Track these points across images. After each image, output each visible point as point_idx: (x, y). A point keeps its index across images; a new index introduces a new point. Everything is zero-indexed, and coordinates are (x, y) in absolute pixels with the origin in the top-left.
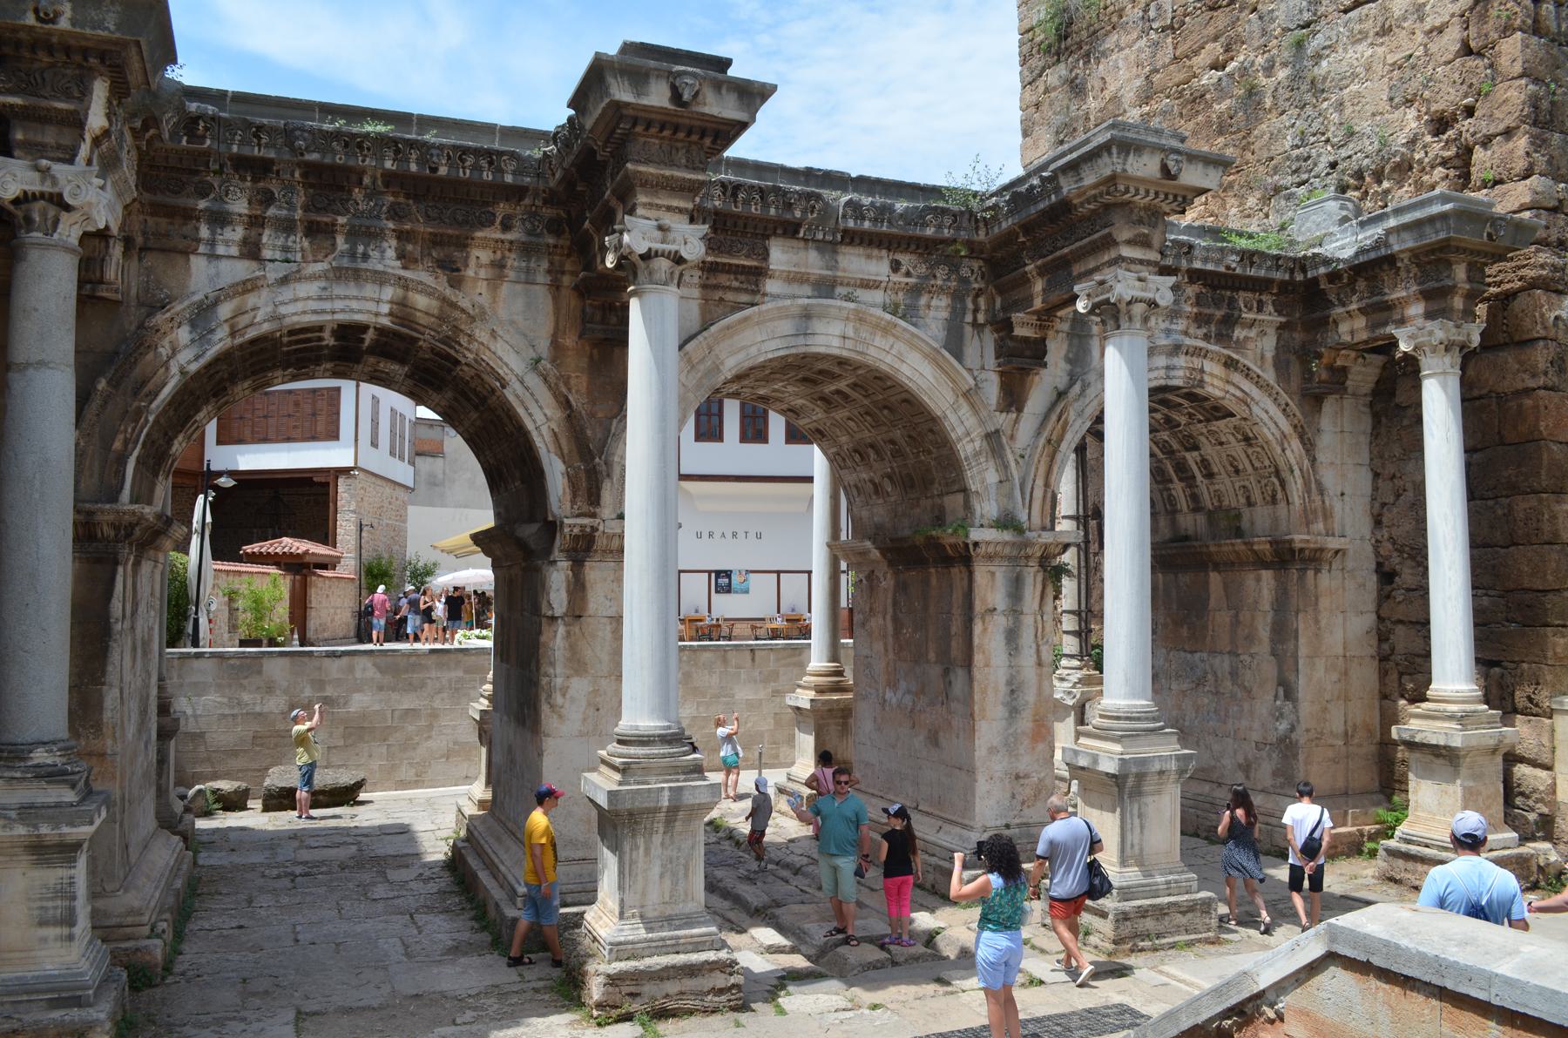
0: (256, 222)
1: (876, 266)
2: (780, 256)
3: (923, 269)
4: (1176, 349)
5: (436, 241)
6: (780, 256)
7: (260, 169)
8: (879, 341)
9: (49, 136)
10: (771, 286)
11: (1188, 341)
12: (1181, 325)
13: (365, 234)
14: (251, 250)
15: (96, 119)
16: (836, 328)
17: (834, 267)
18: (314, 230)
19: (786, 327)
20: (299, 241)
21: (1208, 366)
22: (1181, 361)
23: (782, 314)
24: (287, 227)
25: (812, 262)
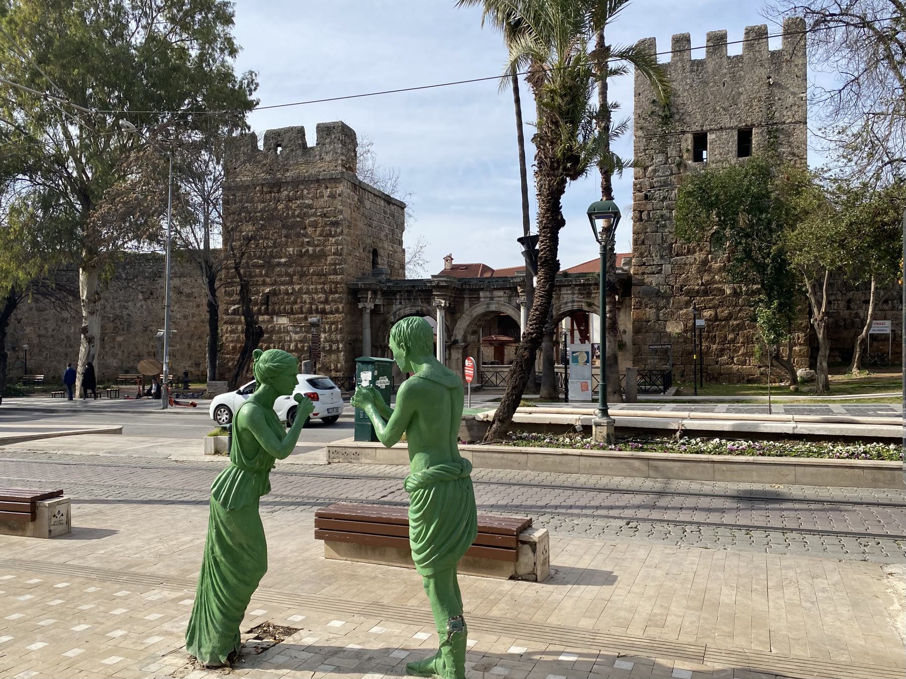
0: (401, 299)
1: (501, 293)
2: (482, 294)
3: (510, 293)
4: (573, 301)
5: (426, 299)
6: (482, 294)
7: (400, 291)
8: (503, 307)
9: (364, 300)
10: (481, 300)
11: (576, 299)
12: (576, 295)
13: (416, 299)
14: (401, 303)
15: (369, 296)
16: (494, 306)
17: (492, 294)
18: (408, 299)
19: (485, 306)
20: (407, 301)
21: (583, 304)
22: (576, 304)
23: (483, 304)
24: (405, 299)
25: (488, 294)
